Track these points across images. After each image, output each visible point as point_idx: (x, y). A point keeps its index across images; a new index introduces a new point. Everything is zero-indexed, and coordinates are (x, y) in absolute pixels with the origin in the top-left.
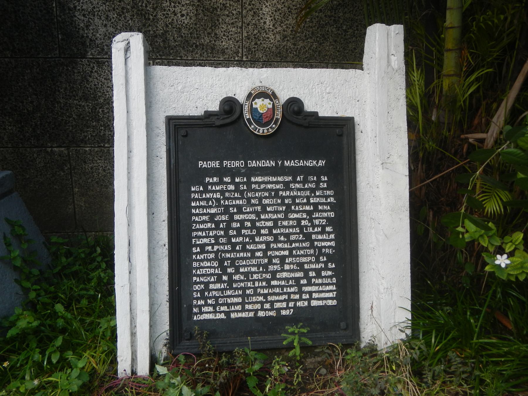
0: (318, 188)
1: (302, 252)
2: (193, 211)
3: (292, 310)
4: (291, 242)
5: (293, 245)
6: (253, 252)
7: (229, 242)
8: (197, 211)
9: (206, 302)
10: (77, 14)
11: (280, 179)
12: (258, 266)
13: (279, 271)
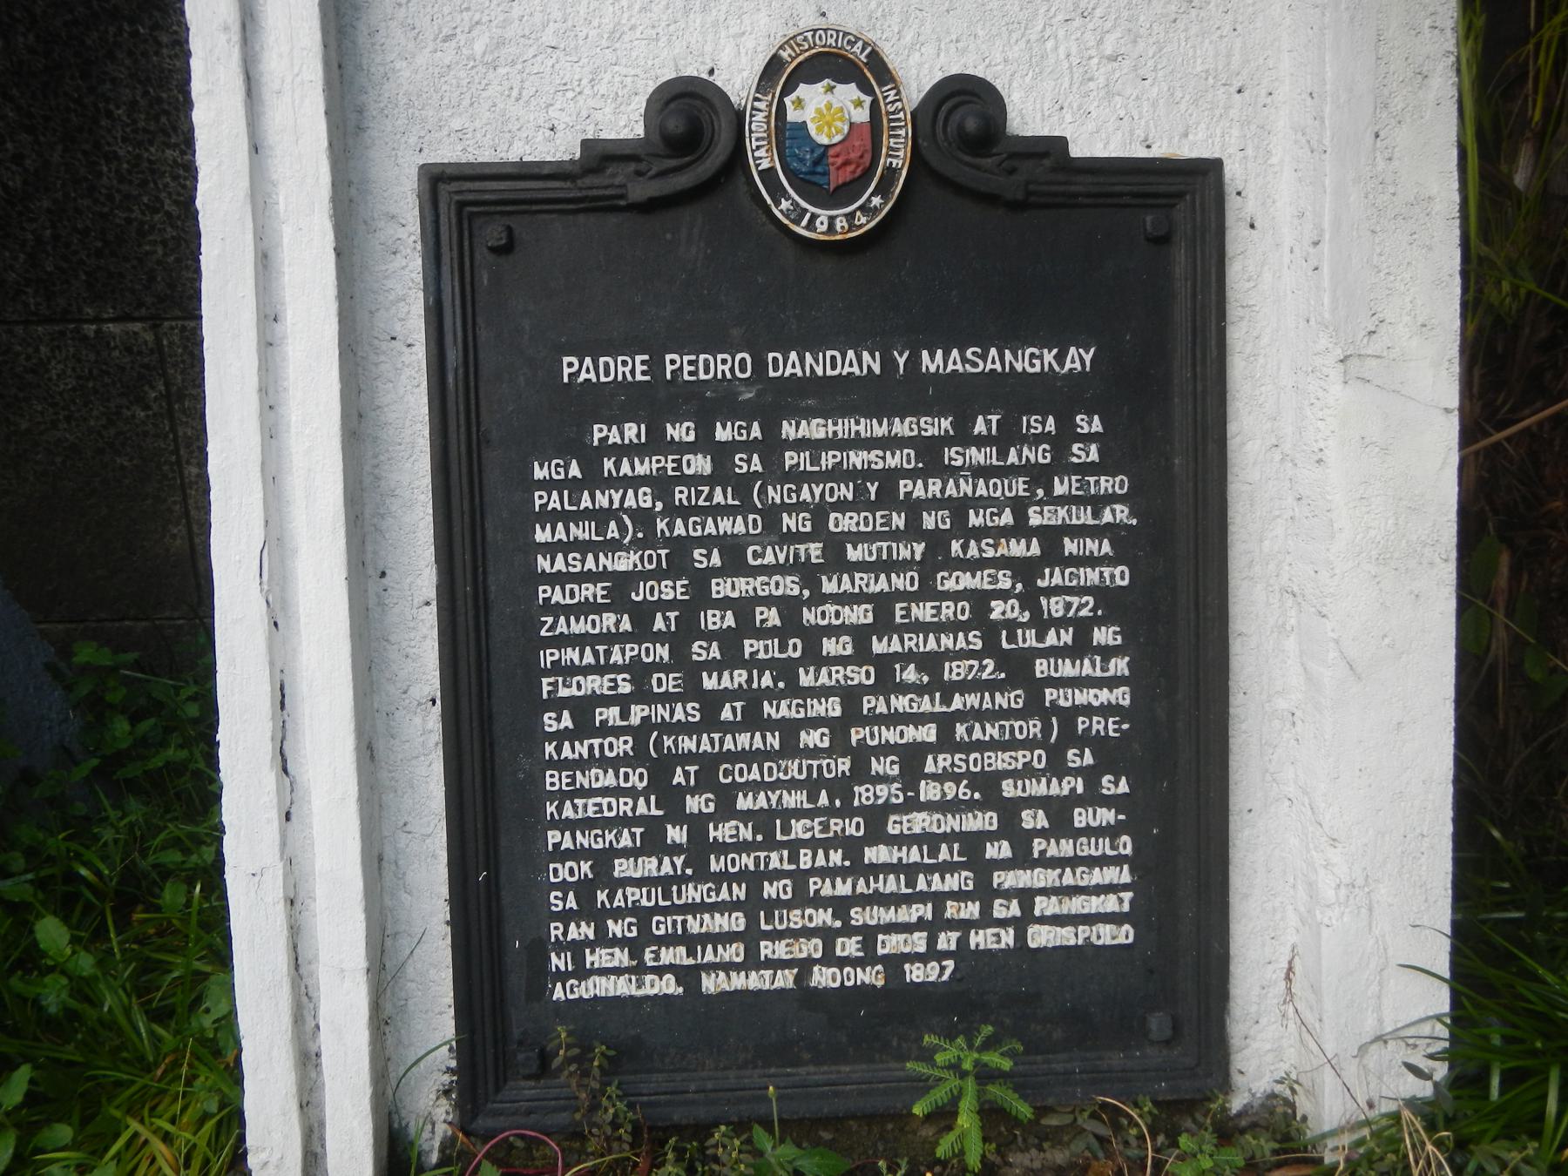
0: (1062, 465)
1: (993, 731)
2: (543, 564)
3: (950, 964)
4: (948, 691)
5: (957, 703)
6: (789, 730)
7: (692, 690)
8: (560, 564)
9: (601, 931)
12: (812, 786)
13: (897, 809)
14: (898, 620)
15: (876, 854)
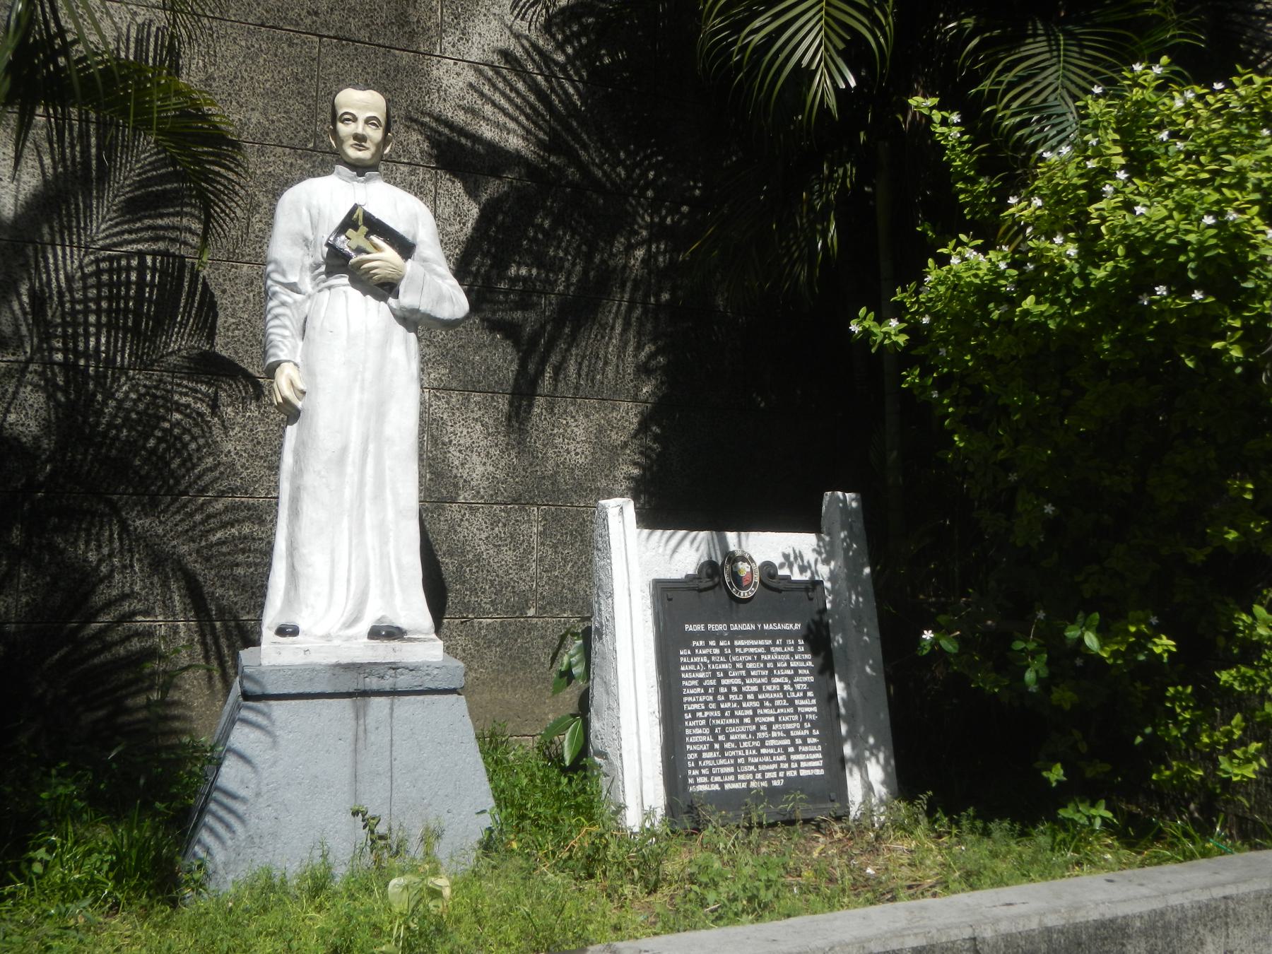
0: (796, 652)
4: (776, 708)
6: (741, 718)
7: (718, 708)
10: (452, 449)
11: (761, 642)
12: (747, 733)
15: (763, 751)
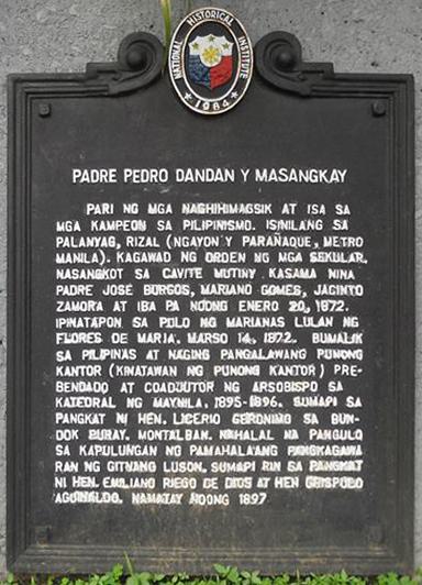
0: (328, 231)
1: (289, 371)
3: (264, 495)
4: (266, 348)
5: (271, 355)
6: (182, 365)
7: (132, 343)
8: (68, 275)
9: (81, 467)
11: (245, 209)
12: (193, 396)
13: (238, 410)
14: (241, 310)
15: (226, 434)
